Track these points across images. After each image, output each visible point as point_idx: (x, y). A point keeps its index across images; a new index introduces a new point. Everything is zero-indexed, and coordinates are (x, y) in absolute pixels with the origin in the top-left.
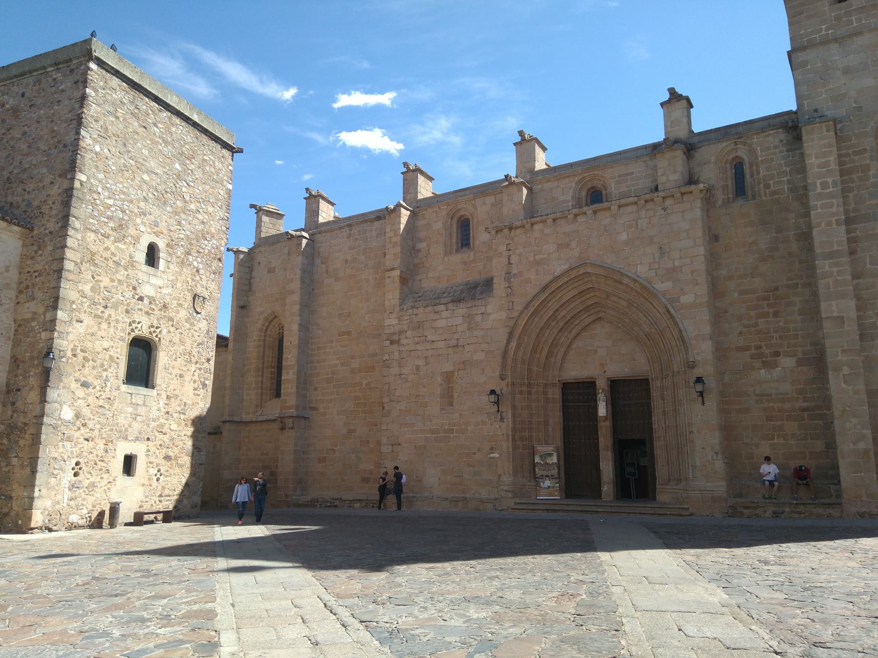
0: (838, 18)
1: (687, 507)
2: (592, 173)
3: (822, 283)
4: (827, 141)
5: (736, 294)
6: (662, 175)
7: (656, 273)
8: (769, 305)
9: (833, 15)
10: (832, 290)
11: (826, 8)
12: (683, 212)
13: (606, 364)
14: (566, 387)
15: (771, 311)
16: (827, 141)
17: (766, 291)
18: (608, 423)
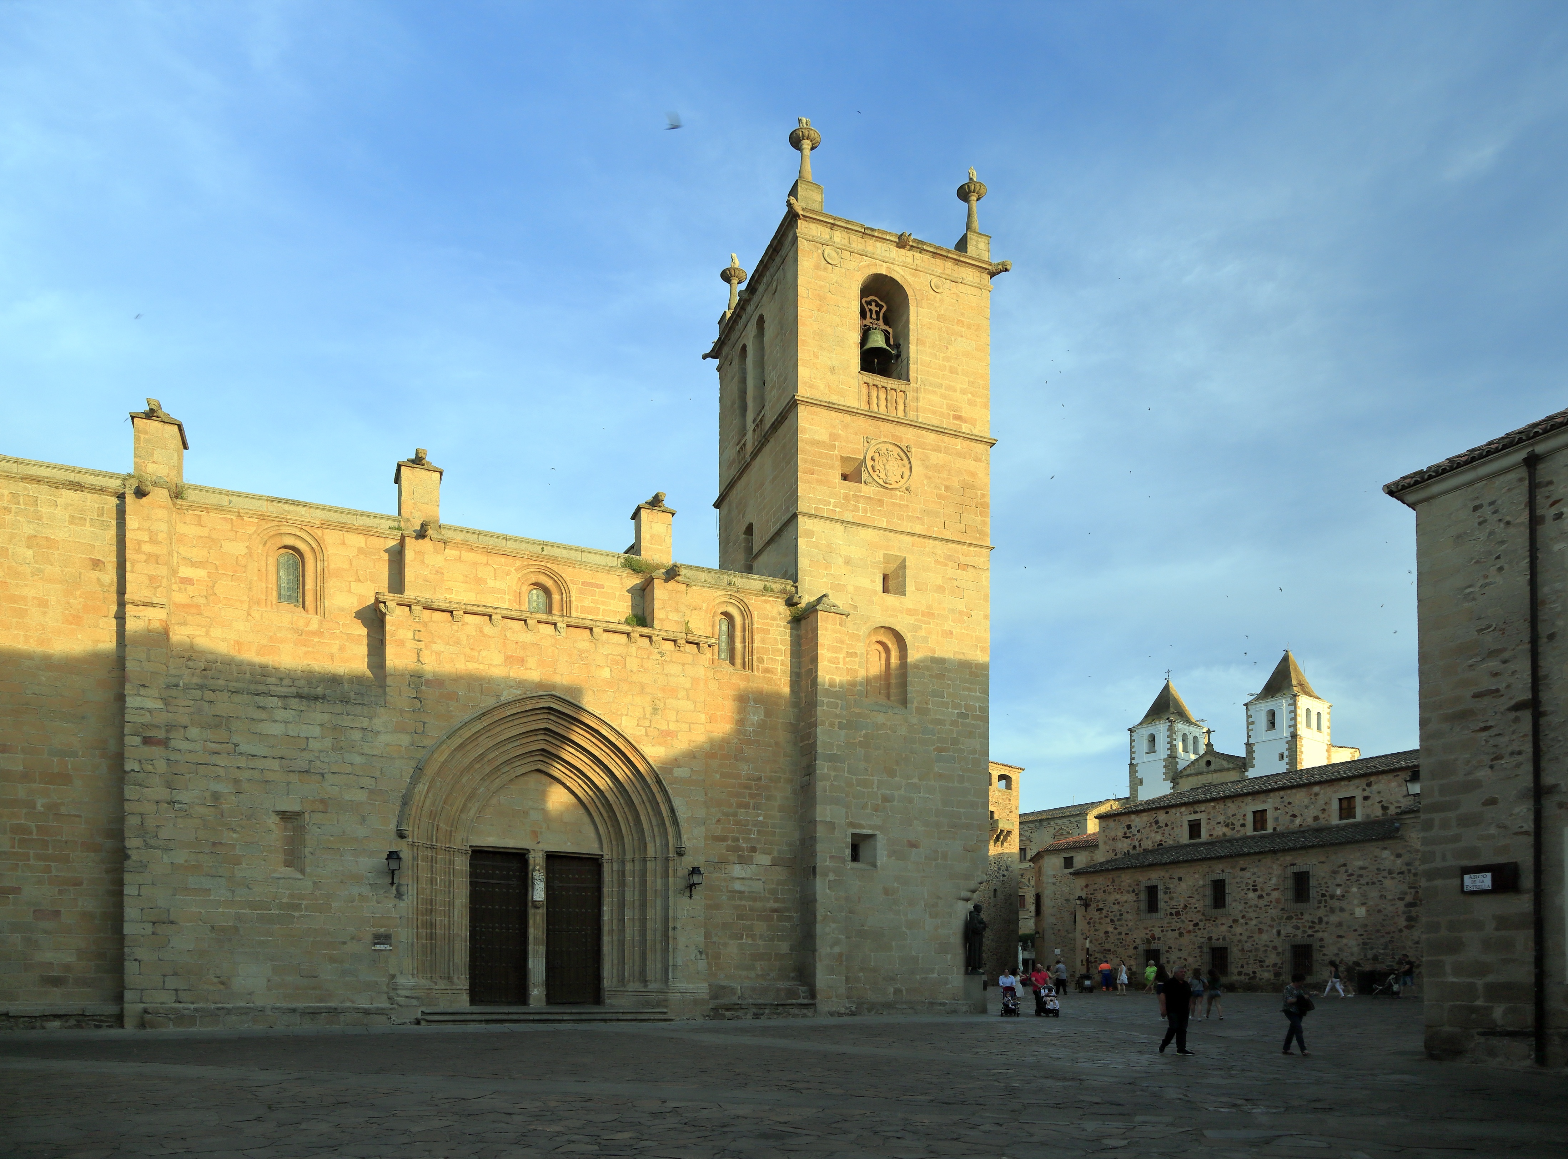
0: (846, 497)
1: (665, 1010)
2: (543, 564)
3: (820, 785)
4: (838, 635)
5: (718, 776)
6: (659, 609)
7: (646, 732)
8: (751, 796)
9: (843, 491)
10: (828, 793)
11: (837, 481)
12: (684, 665)
13: (541, 833)
14: (479, 855)
15: (752, 802)
16: (838, 635)
17: (749, 779)
18: (543, 911)
